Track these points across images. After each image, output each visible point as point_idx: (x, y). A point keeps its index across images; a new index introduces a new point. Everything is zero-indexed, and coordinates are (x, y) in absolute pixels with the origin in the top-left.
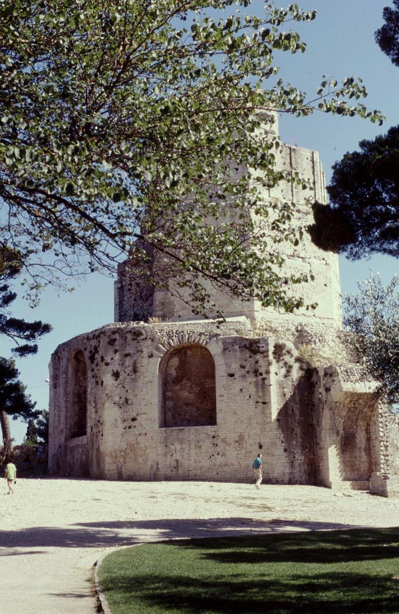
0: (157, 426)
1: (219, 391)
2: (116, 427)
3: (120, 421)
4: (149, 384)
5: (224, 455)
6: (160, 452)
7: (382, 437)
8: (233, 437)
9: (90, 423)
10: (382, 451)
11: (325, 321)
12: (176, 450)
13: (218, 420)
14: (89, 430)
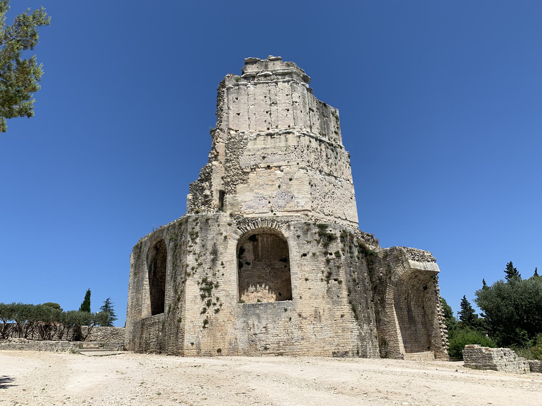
0: (236, 301)
1: (294, 268)
2: (196, 304)
3: (200, 297)
4: (228, 263)
5: (300, 328)
6: (238, 327)
7: (438, 312)
8: (307, 311)
9: (168, 301)
10: (440, 324)
11: (354, 224)
12: (254, 325)
13: (293, 296)
14: (167, 309)
